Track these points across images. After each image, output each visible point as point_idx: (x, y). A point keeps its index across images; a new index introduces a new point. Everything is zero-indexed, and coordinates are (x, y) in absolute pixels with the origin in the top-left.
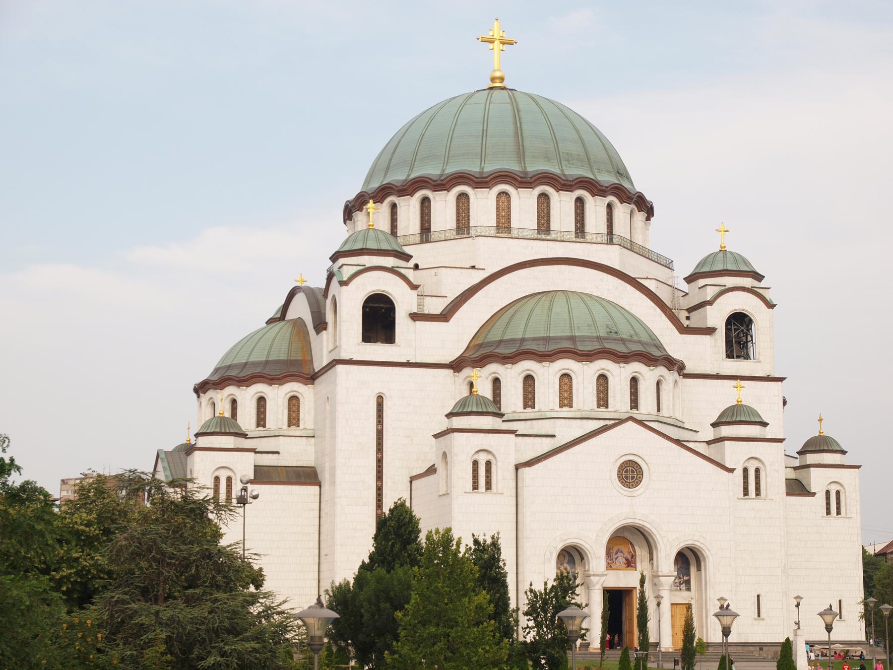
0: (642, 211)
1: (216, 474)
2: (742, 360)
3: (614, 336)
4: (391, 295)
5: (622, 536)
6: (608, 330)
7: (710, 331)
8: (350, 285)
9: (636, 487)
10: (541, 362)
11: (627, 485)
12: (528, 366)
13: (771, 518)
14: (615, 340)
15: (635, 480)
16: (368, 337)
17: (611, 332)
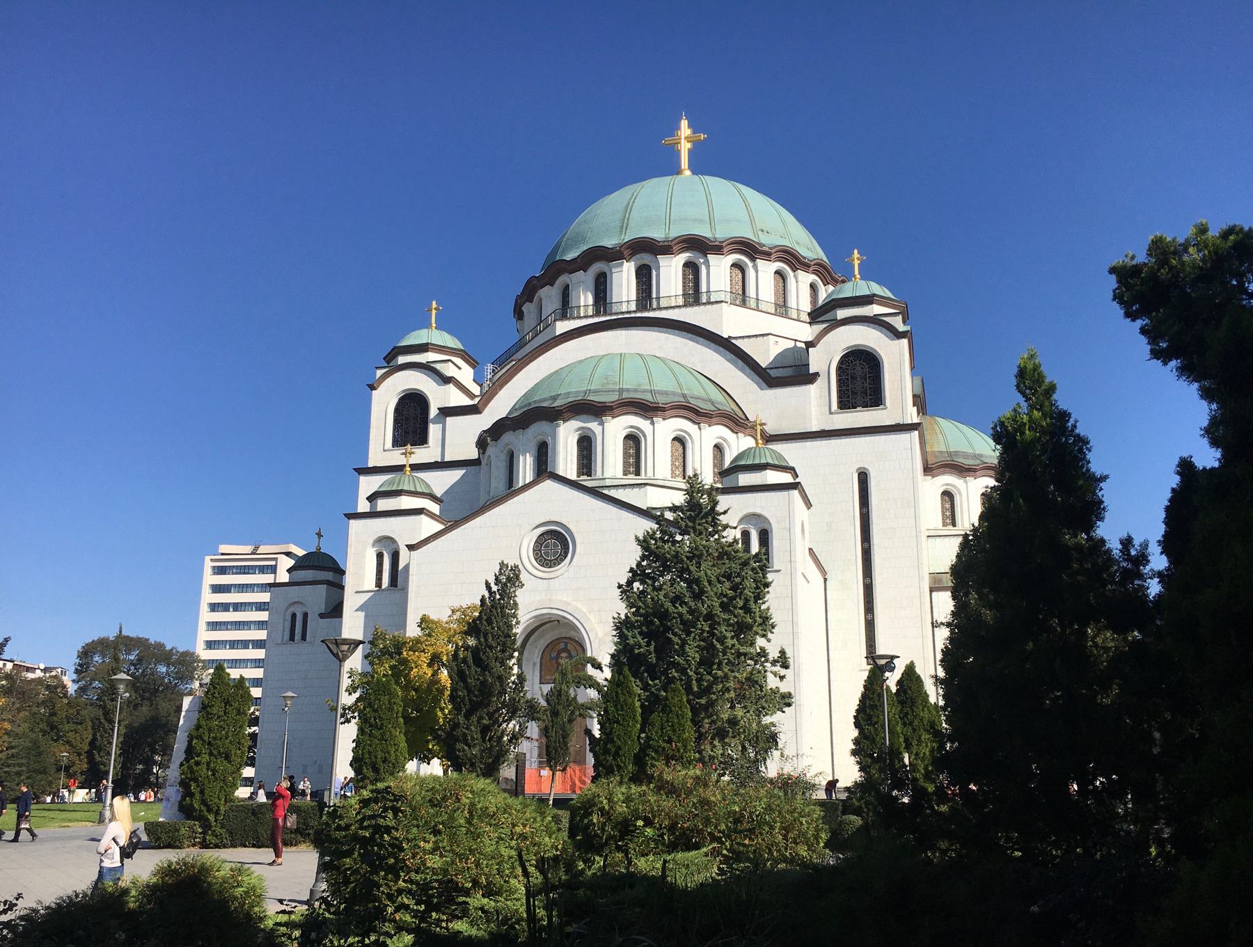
0: (798, 269)
1: (292, 610)
2: (858, 409)
3: (611, 386)
4: (423, 392)
5: (567, 636)
6: (605, 381)
7: (811, 378)
8: (379, 388)
9: (559, 564)
10: (514, 430)
11: (547, 564)
12: (508, 437)
13: (778, 597)
14: (609, 391)
15: (558, 557)
16: (399, 441)
17: (608, 384)
